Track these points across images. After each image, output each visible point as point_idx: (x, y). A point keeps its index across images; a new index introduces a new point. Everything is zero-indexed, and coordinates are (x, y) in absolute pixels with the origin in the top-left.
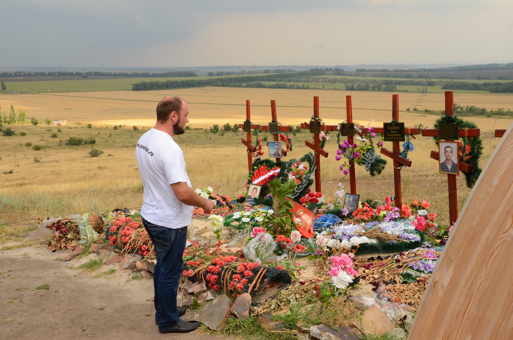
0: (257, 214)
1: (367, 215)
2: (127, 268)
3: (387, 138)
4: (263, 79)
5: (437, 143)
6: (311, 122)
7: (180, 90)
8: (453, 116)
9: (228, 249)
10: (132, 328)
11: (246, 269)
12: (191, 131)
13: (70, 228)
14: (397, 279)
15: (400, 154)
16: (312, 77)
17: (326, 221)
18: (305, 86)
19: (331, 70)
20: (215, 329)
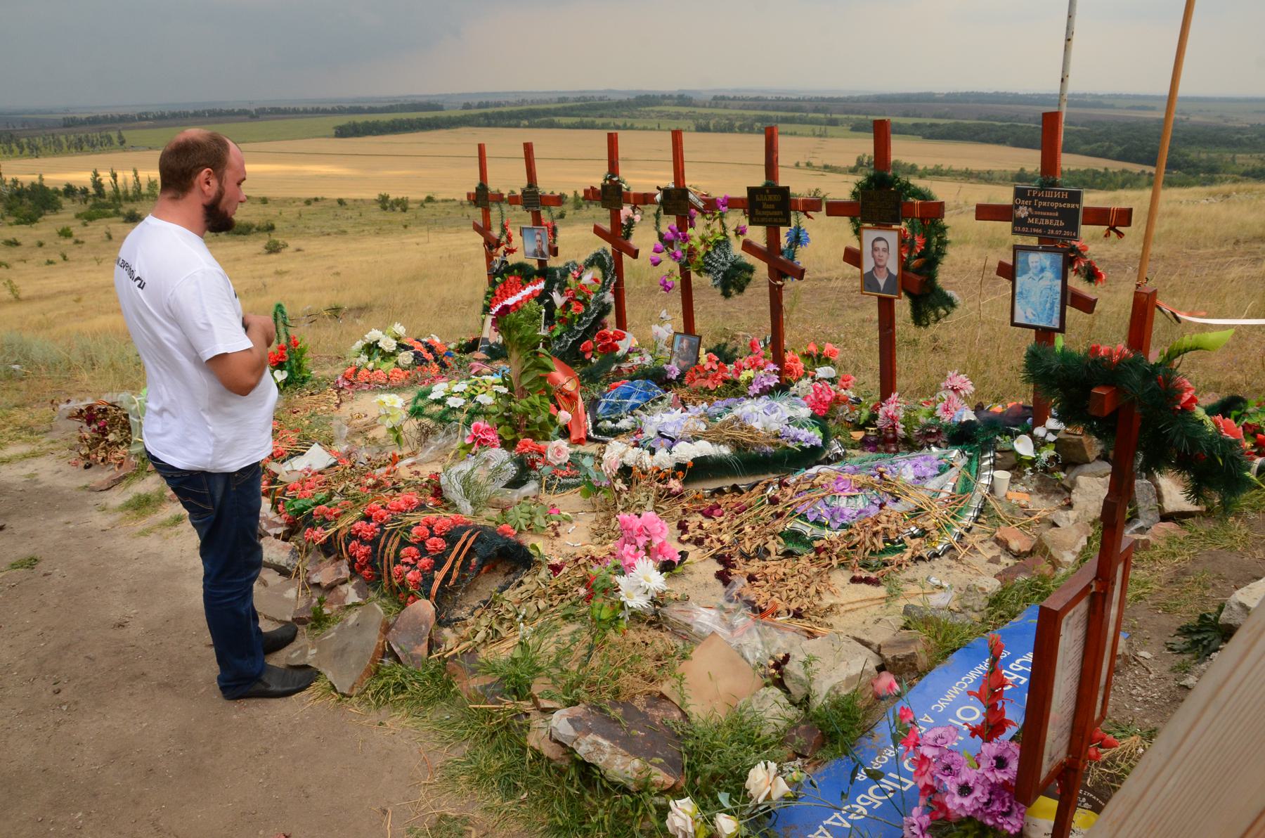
0: (481, 387)
1: (714, 378)
3: (754, 220)
4: (556, 113)
5: (857, 232)
6: (603, 186)
7: (416, 134)
8: (890, 173)
9: (414, 469)
10: (167, 685)
11: (432, 535)
12: (436, 205)
13: (114, 418)
14: (772, 546)
15: (782, 253)
17: (628, 396)
18: (628, 125)
19: (670, 97)
20: (346, 691)
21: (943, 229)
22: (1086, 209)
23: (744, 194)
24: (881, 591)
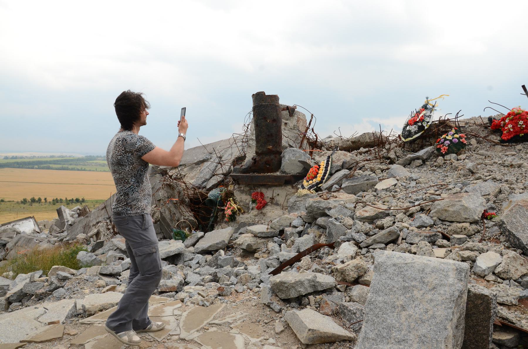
4: (50, 162)
12: (6, 203)
16: (87, 162)
18: (83, 169)
19: (100, 157)
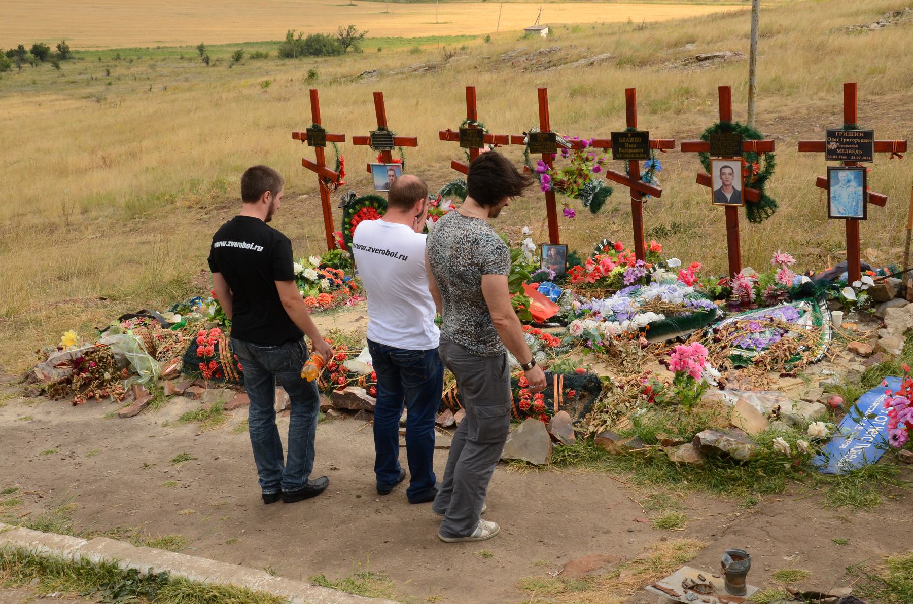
2: (284, 410)
3: (618, 156)
6: (461, 130)
15: (641, 178)
21: (772, 157)
22: (877, 143)
23: (609, 138)
24: (799, 380)
